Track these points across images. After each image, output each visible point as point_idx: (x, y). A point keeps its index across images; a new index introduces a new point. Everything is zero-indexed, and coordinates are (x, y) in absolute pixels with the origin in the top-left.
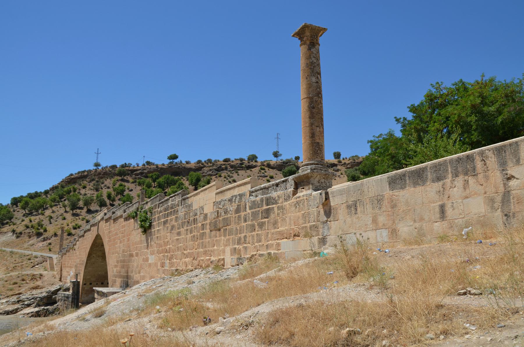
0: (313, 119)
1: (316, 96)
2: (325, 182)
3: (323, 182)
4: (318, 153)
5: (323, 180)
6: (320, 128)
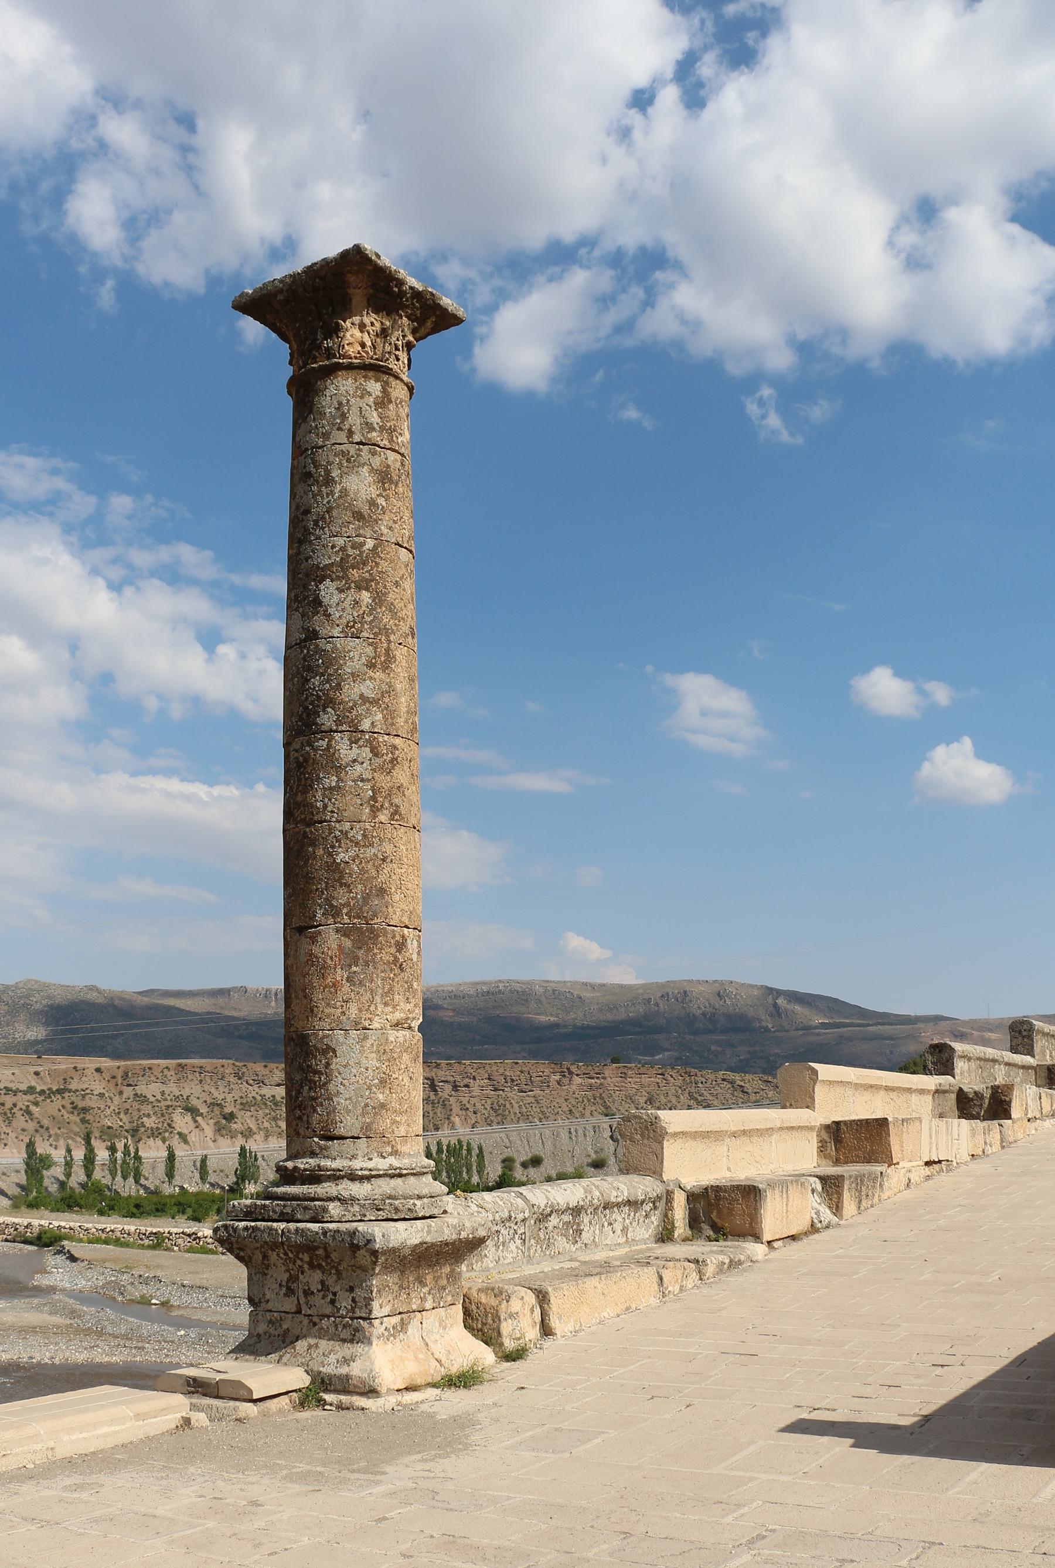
2: (324, 1287)
3: (315, 1287)
5: (314, 1279)
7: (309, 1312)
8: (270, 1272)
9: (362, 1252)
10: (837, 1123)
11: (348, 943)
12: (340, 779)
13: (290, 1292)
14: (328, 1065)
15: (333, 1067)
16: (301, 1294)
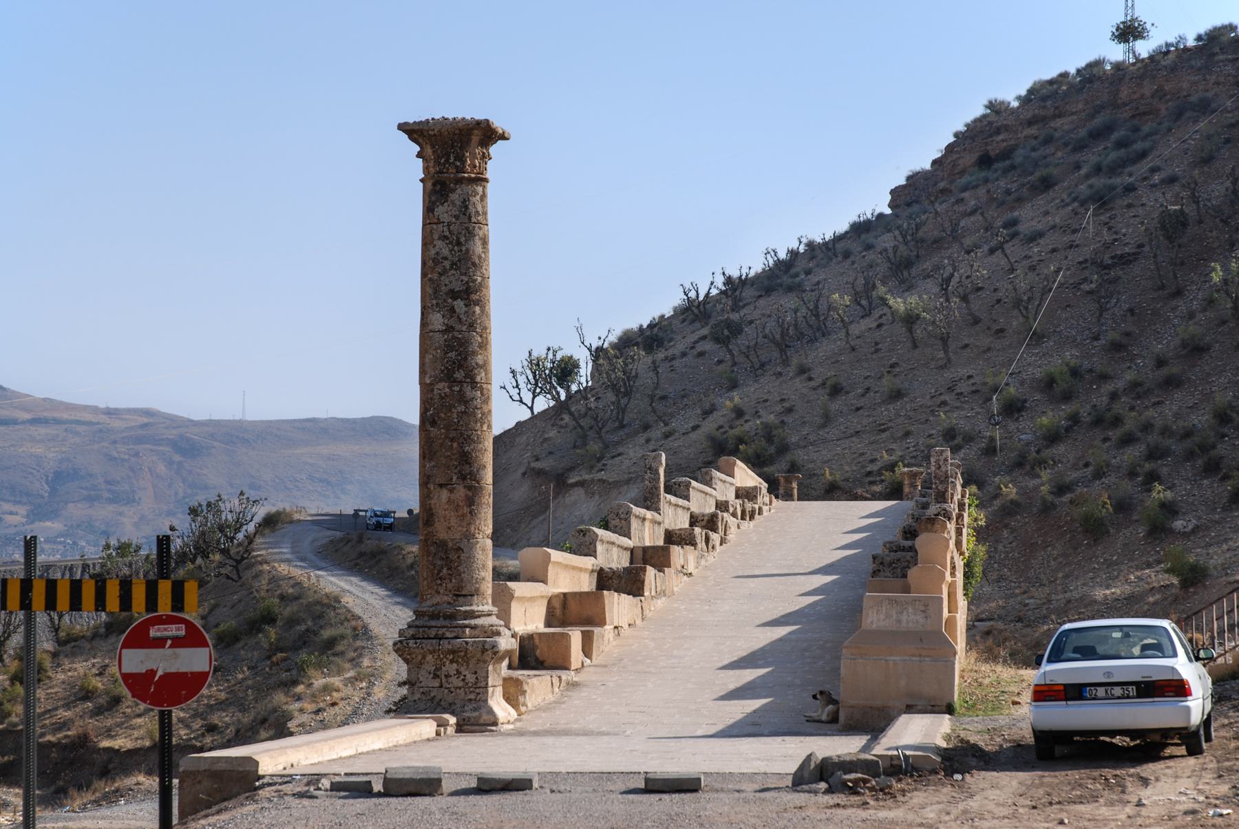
0: (431, 460)
1: (441, 380)
2: (458, 672)
3: (453, 672)
4: (441, 579)
5: (451, 668)
6: (451, 491)
7: (448, 686)
8: (423, 666)
9: (489, 652)
10: (565, 594)
11: (470, 494)
12: (467, 407)
13: (436, 676)
14: (459, 557)
15: (461, 558)
16: (443, 677)
